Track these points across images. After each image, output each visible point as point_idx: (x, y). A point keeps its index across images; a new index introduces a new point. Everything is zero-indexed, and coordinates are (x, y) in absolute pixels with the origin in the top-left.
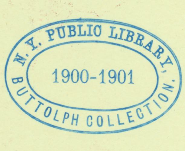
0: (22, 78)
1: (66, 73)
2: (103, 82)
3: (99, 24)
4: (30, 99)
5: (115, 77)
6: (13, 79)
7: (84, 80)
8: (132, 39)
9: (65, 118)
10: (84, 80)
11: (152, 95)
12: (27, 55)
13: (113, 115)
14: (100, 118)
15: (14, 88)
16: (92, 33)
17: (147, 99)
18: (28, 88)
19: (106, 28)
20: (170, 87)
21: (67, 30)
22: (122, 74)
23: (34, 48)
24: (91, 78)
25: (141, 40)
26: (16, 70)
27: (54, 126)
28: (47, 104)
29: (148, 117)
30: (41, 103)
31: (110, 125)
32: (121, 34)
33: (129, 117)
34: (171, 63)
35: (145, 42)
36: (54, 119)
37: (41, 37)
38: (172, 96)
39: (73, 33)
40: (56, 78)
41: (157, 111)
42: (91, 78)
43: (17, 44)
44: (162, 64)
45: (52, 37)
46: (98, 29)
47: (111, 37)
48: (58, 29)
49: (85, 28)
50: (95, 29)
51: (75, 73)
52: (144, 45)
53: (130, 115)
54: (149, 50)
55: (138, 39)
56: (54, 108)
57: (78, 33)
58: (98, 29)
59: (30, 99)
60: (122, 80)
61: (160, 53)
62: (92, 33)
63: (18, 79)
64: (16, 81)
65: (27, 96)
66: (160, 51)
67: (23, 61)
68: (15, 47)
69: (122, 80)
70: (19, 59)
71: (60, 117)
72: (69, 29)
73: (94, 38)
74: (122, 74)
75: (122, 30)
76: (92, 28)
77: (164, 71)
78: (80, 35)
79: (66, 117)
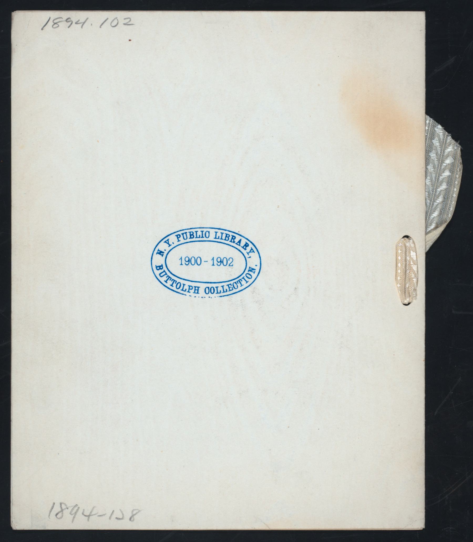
8: (228, 239)
16: (204, 236)
23: (170, 245)
26: (159, 260)
35: (237, 240)
37: (173, 239)
43: (158, 244)
44: (248, 253)
45: (180, 239)
46: (207, 233)
47: (216, 238)
48: (183, 234)
52: (236, 242)
54: (239, 245)
55: (232, 238)
57: (195, 236)
58: (207, 233)
62: (204, 236)
66: (246, 245)
68: (157, 245)
70: (160, 253)
72: (191, 235)
73: (205, 239)
75: (222, 233)
77: (250, 257)
78: (197, 237)
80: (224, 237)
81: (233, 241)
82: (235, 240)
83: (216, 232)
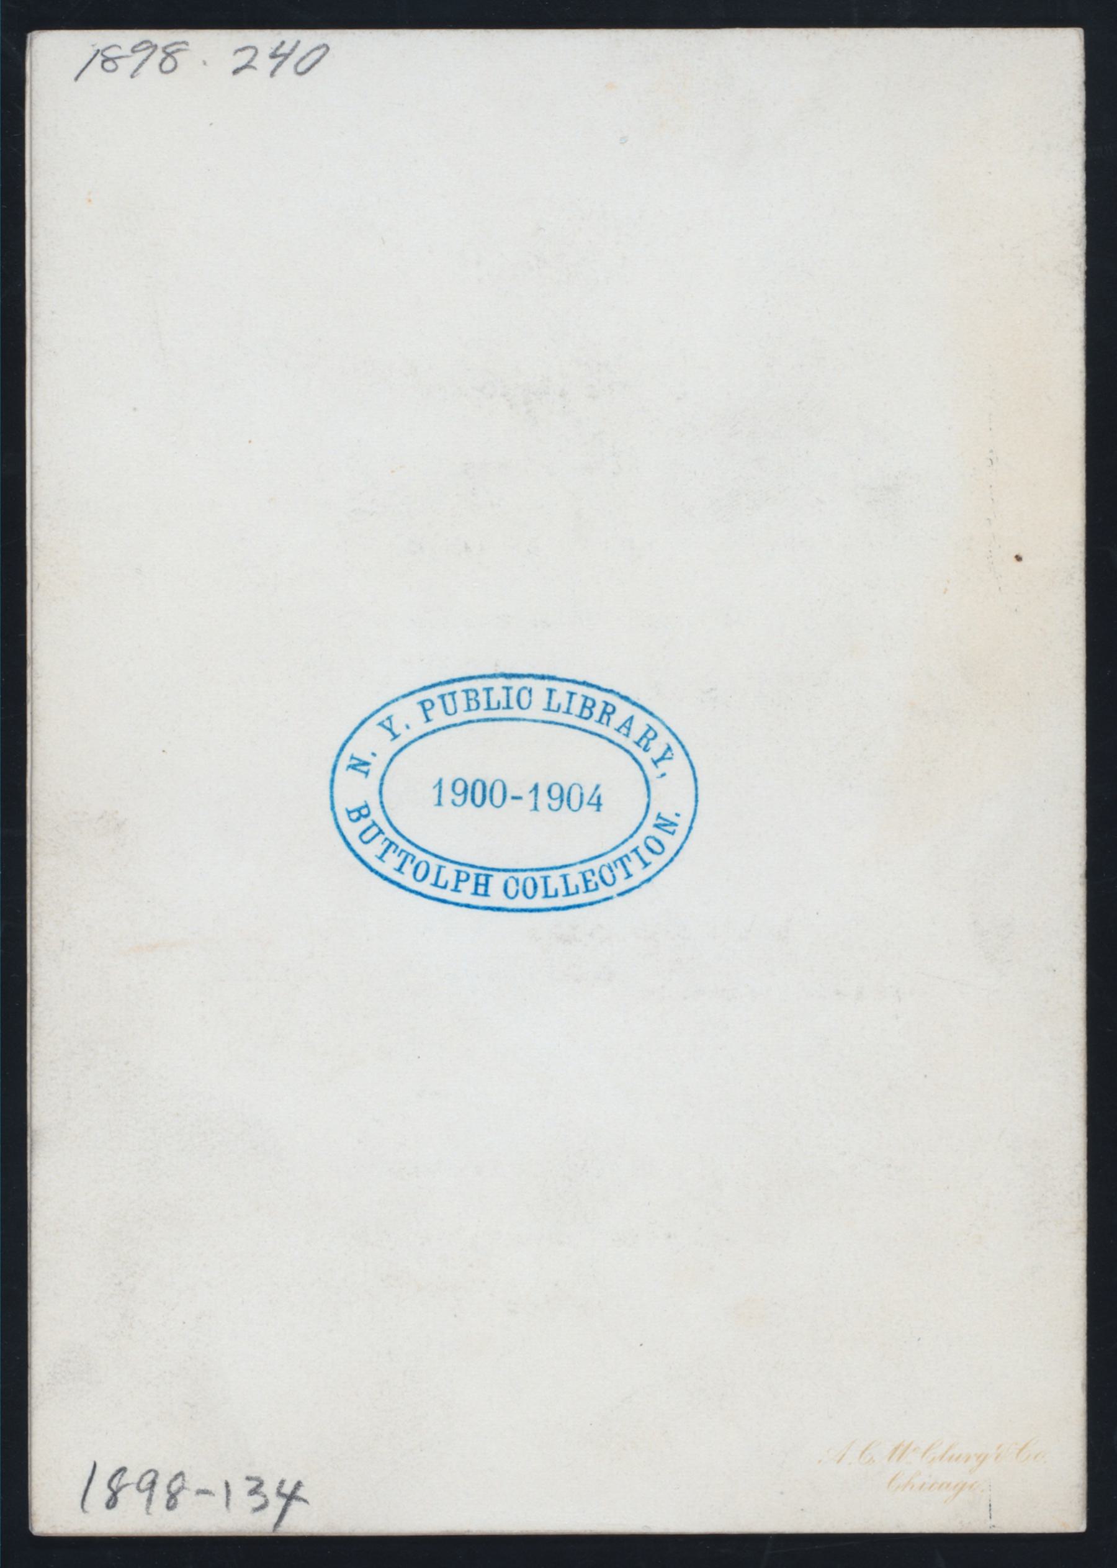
1: (460, 787)
16: (513, 703)
21: (461, 698)
35: (617, 720)
37: (407, 714)
39: (473, 705)
44: (655, 763)
48: (442, 697)
49: (498, 695)
55: (604, 712)
58: (525, 696)
62: (513, 703)
73: (516, 712)
76: (513, 694)
77: (663, 775)
78: (489, 708)
83: (551, 691)
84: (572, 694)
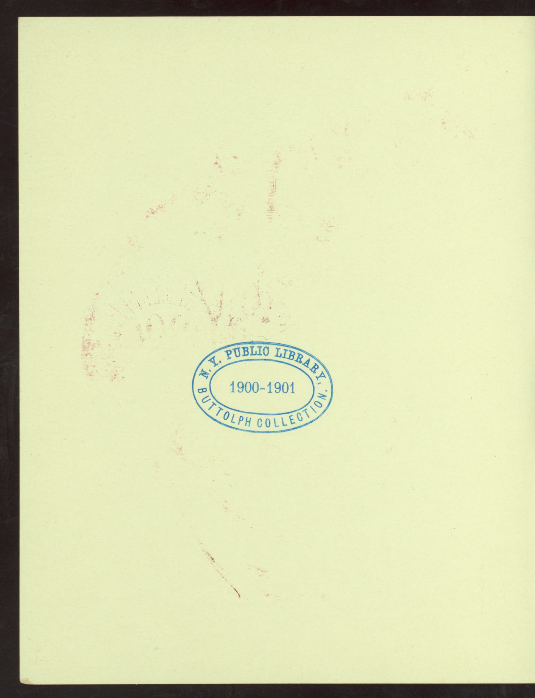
0: (206, 389)
1: (241, 385)
2: (270, 392)
3: (267, 346)
4: (212, 406)
5: (280, 388)
6: (199, 390)
7: (256, 390)
8: (294, 357)
9: (240, 420)
10: (256, 390)
11: (309, 403)
12: (210, 371)
13: (278, 418)
14: (268, 421)
15: (200, 397)
16: (262, 353)
17: (306, 406)
18: (211, 397)
19: (273, 349)
20: (324, 396)
21: (242, 350)
22: (285, 385)
23: (215, 365)
24: (261, 389)
25: (300, 359)
27: (231, 427)
28: (226, 410)
29: (306, 420)
30: (221, 409)
31: (276, 426)
32: (285, 354)
33: (291, 420)
34: (324, 376)
35: (304, 360)
36: (232, 421)
37: (221, 356)
38: (325, 403)
39: (246, 353)
40: (233, 389)
41: (313, 416)
42: (261, 389)
43: (202, 362)
44: (317, 378)
45: (230, 356)
46: (266, 350)
47: (277, 356)
48: (235, 350)
49: (256, 349)
50: (264, 350)
51: (248, 385)
52: (303, 363)
53: (292, 418)
54: (307, 366)
55: (298, 357)
56: (232, 412)
57: (250, 353)
58: (266, 350)
59: (212, 406)
60: (285, 390)
61: (316, 369)
62: (262, 353)
63: (203, 389)
64: (201, 391)
65: (210, 403)
66: (316, 367)
67: (206, 376)
68: (200, 364)
69: (285, 391)
71: (236, 419)
72: (243, 350)
74: (285, 385)
75: (286, 350)
76: (262, 349)
78: (252, 354)
79: (241, 419)
80: (287, 355)
81: (299, 360)
82: (302, 360)
83: (278, 349)
84: (286, 350)
